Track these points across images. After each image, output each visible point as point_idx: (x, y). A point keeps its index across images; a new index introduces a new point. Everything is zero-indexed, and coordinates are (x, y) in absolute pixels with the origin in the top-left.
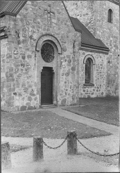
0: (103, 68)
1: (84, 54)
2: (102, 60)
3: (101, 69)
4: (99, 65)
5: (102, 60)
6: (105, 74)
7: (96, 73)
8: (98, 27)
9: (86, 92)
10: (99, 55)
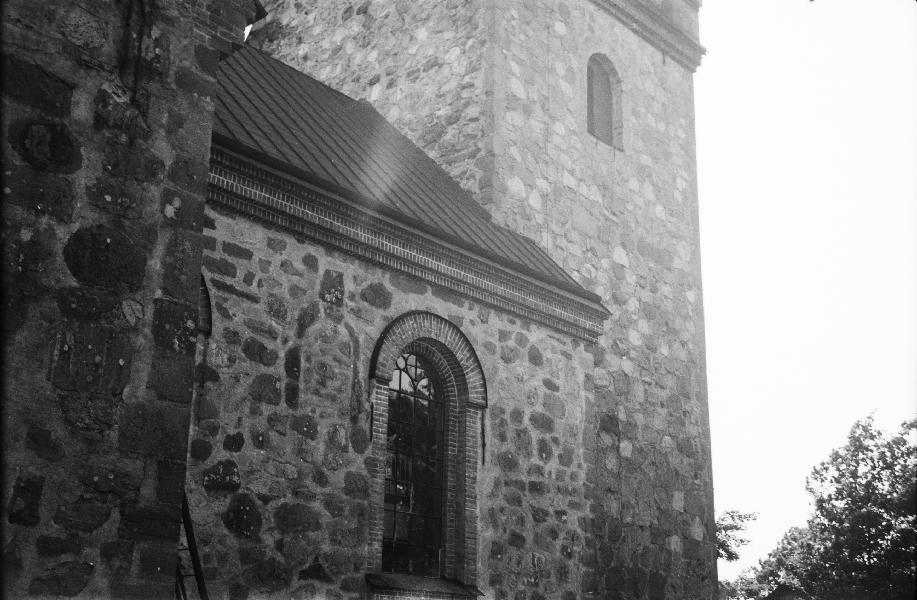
0: (556, 451)
1: (377, 296)
2: (549, 384)
3: (535, 460)
5: (549, 384)
6: (573, 505)
7: (497, 484)
8: (514, 151)
10: (522, 340)
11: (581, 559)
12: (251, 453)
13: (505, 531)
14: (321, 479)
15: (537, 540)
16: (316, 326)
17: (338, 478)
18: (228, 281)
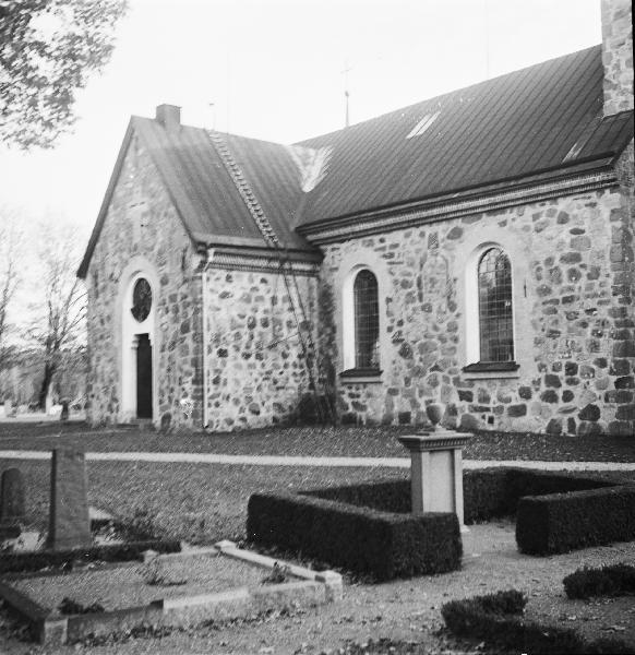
4: (557, 262)
9: (475, 402)
11: (612, 336)
12: (406, 326)
13: (543, 330)
14: (436, 328)
15: (570, 330)
16: (427, 263)
17: (443, 327)
18: (392, 260)
